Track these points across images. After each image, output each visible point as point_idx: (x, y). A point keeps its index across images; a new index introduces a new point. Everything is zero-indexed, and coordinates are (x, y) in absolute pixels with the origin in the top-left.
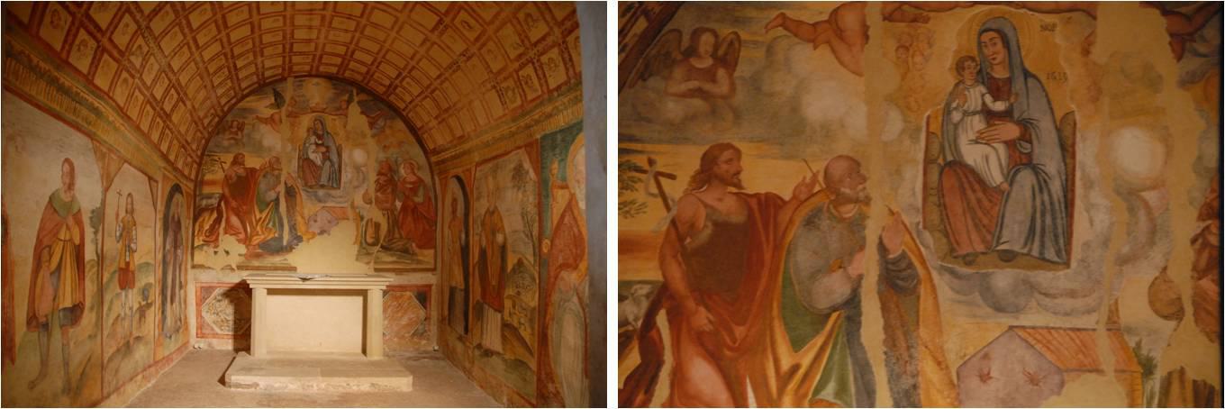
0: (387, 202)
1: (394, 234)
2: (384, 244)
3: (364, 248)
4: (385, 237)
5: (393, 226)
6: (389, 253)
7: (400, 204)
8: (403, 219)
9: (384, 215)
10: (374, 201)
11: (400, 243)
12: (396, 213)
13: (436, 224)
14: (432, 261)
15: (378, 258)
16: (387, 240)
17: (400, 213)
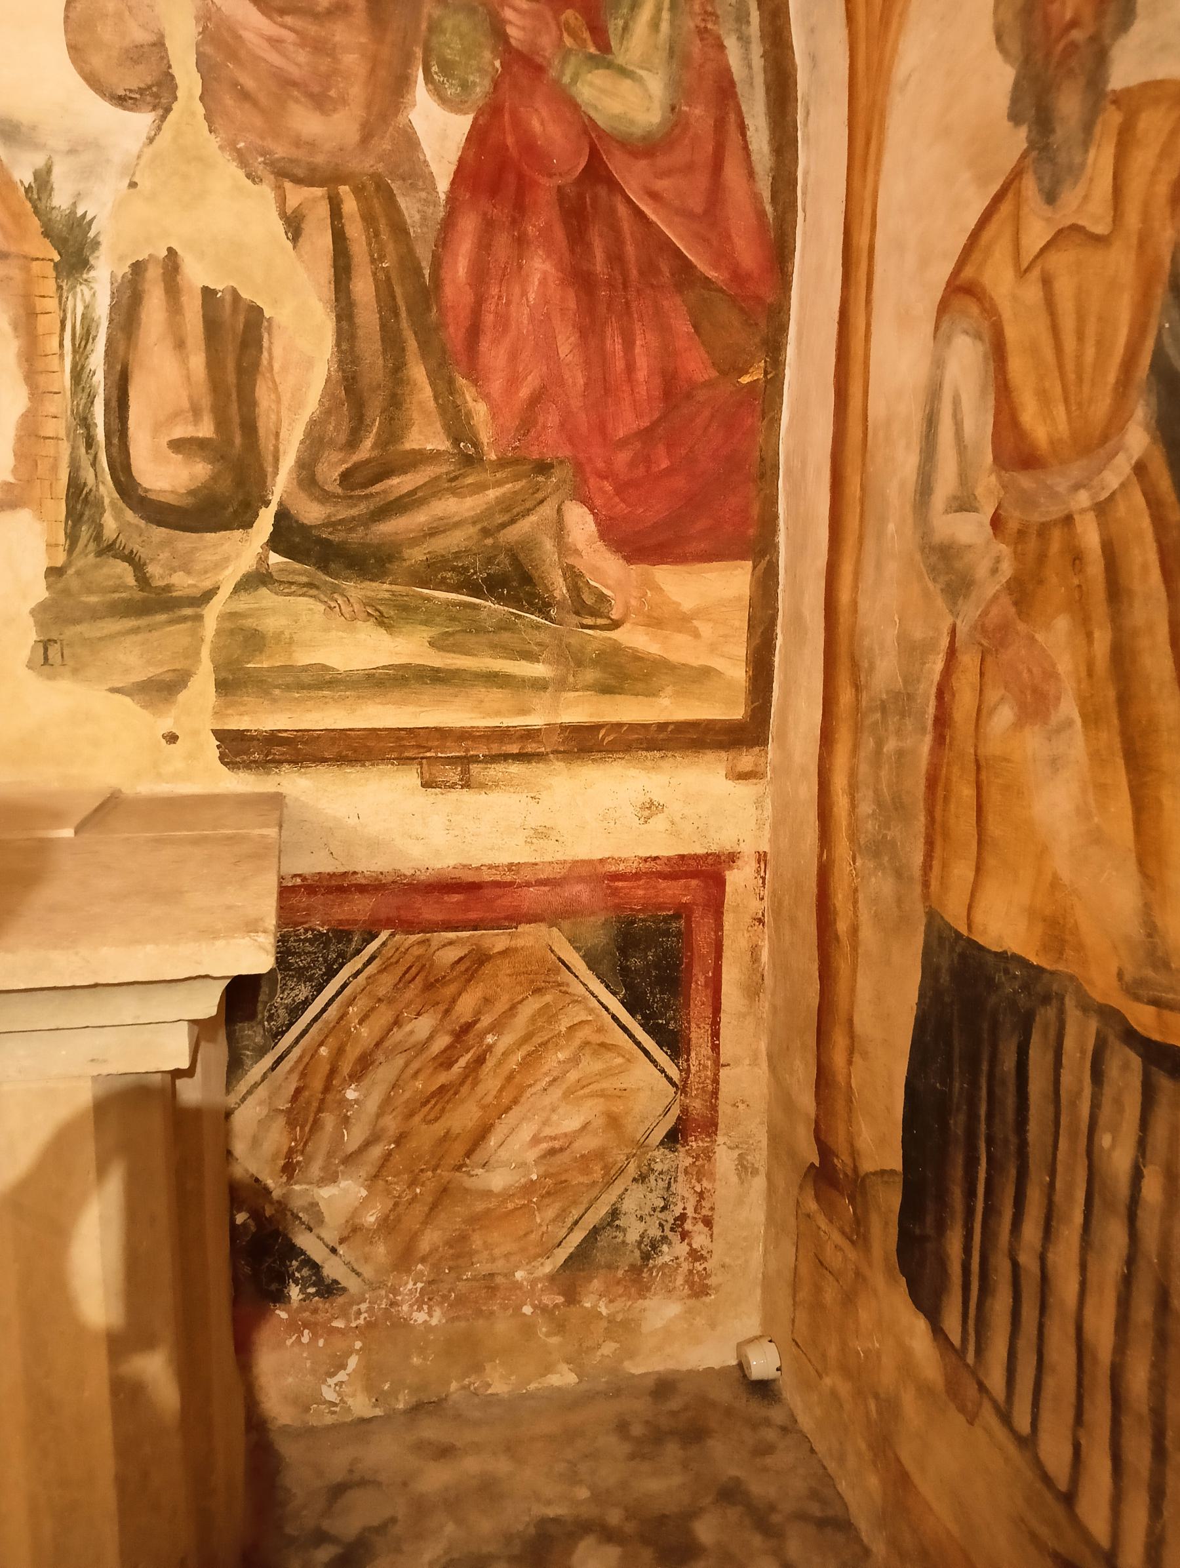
0: (321, 102)
1: (392, 433)
2: (311, 513)
3: (108, 550)
4: (315, 442)
5: (392, 341)
6: (357, 590)
7: (461, 124)
8: (479, 275)
9: (294, 226)
10: (188, 80)
11: (449, 506)
12: (409, 207)
13: (774, 348)
14: (738, 673)
15: (255, 641)
16: (330, 471)
17: (448, 225)
